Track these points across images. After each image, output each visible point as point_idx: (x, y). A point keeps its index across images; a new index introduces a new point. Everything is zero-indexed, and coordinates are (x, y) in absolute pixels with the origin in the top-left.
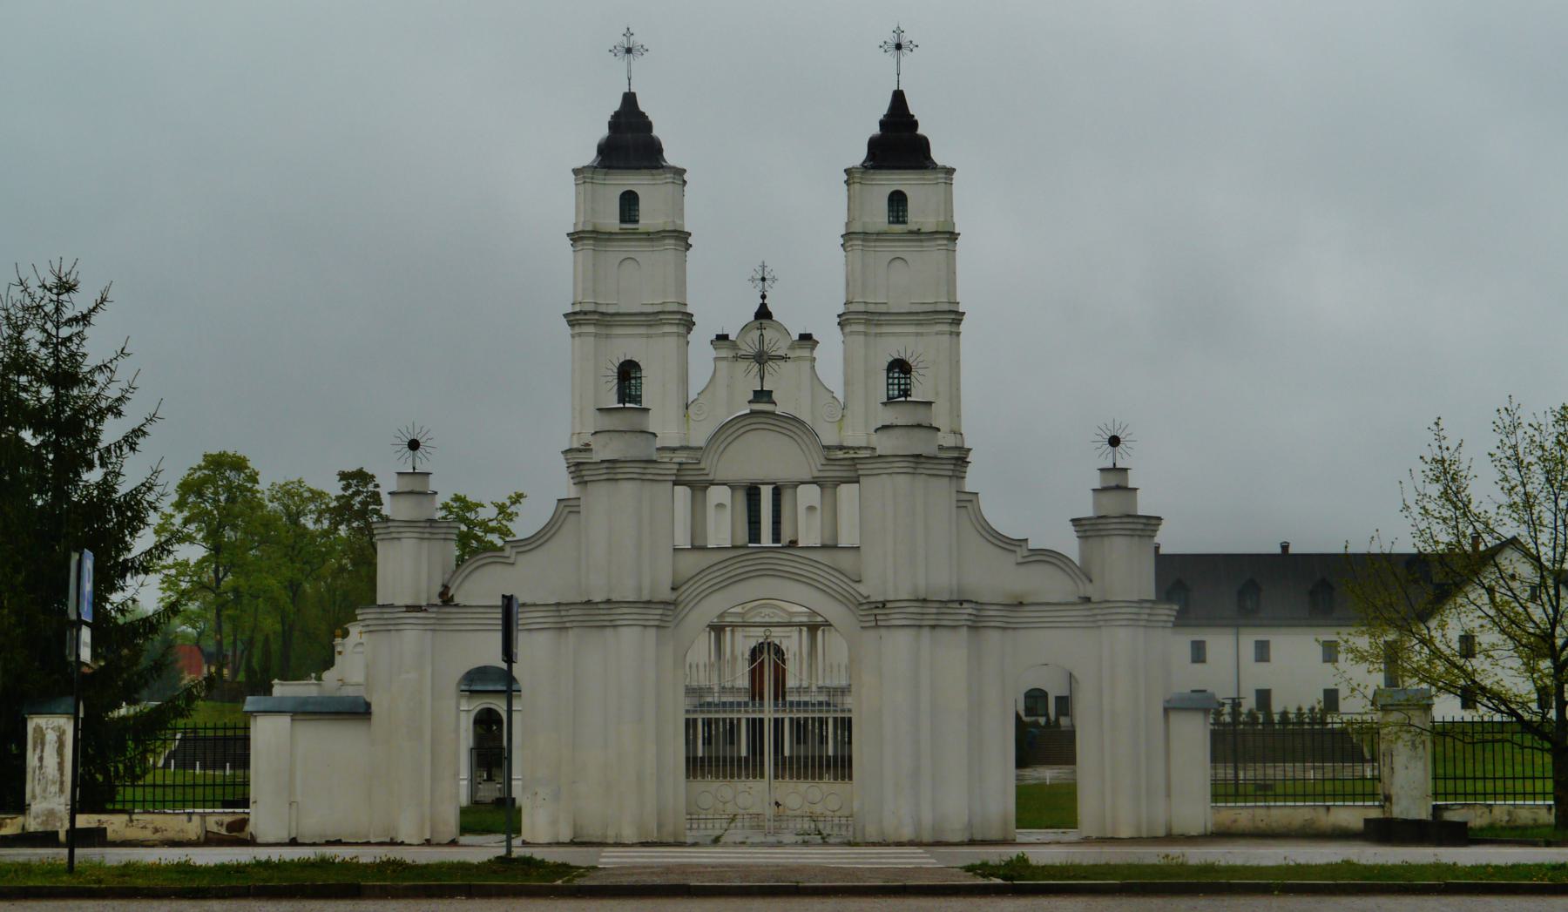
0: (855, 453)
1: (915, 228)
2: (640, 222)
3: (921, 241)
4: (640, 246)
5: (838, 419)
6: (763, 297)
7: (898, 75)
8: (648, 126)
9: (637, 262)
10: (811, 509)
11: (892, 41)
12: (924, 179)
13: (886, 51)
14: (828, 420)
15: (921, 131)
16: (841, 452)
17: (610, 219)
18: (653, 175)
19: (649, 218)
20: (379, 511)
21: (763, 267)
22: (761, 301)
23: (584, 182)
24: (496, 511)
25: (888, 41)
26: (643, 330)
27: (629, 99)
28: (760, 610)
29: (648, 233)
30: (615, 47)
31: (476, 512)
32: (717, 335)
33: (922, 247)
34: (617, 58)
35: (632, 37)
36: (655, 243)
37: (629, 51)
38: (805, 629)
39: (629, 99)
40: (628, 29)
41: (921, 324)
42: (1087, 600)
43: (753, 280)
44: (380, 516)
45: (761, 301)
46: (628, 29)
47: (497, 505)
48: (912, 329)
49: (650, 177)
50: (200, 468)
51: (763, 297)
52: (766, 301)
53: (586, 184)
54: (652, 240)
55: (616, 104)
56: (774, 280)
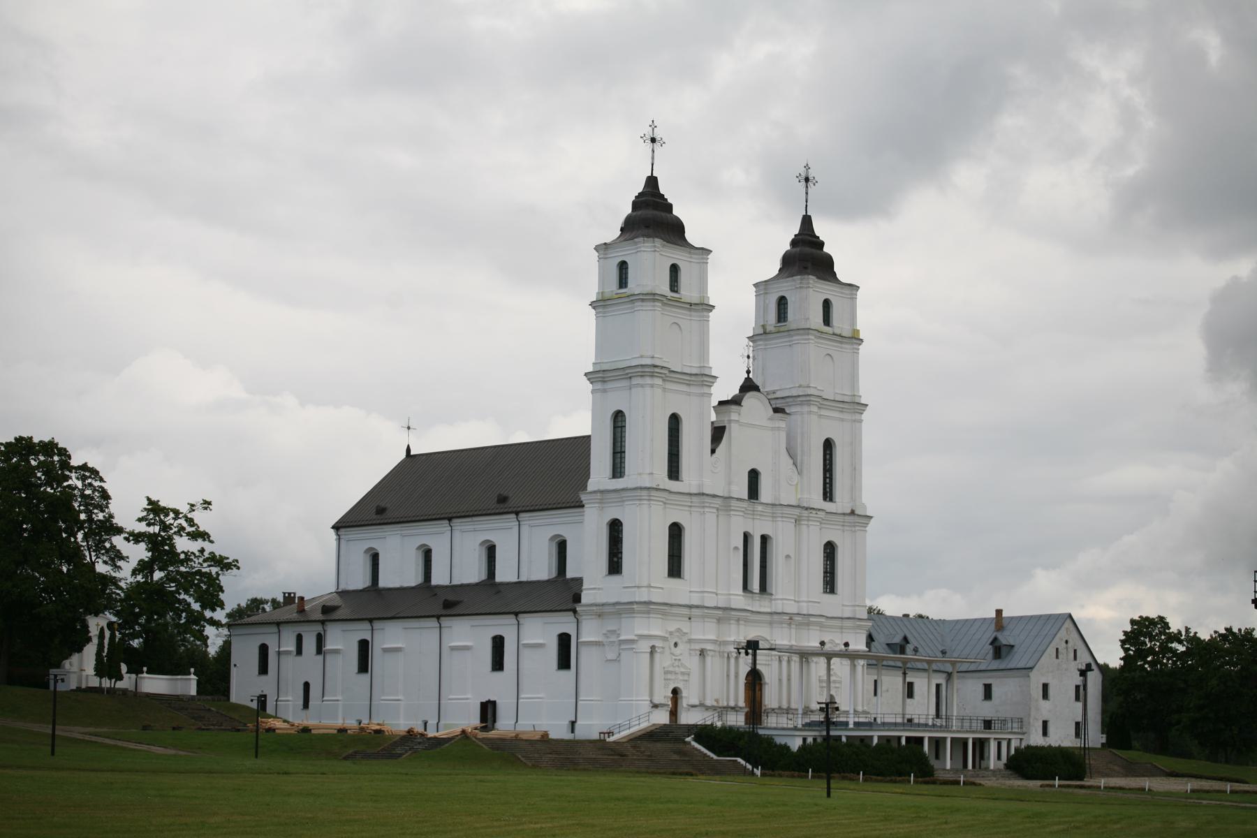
0: (816, 513)
1: (837, 331)
3: (841, 343)
4: (679, 313)
6: (748, 372)
7: (807, 202)
8: (669, 207)
9: (680, 327)
10: (788, 556)
11: (804, 175)
12: (842, 293)
14: (790, 482)
15: (825, 249)
16: (806, 512)
17: (665, 289)
18: (690, 253)
19: (688, 291)
22: (746, 376)
23: (655, 251)
25: (802, 174)
26: (684, 388)
27: (652, 182)
33: (841, 348)
36: (693, 313)
38: (796, 658)
39: (652, 182)
40: (653, 121)
41: (842, 411)
43: (743, 356)
46: (653, 121)
49: (689, 255)
53: (656, 253)
54: (690, 310)
56: (743, 356)
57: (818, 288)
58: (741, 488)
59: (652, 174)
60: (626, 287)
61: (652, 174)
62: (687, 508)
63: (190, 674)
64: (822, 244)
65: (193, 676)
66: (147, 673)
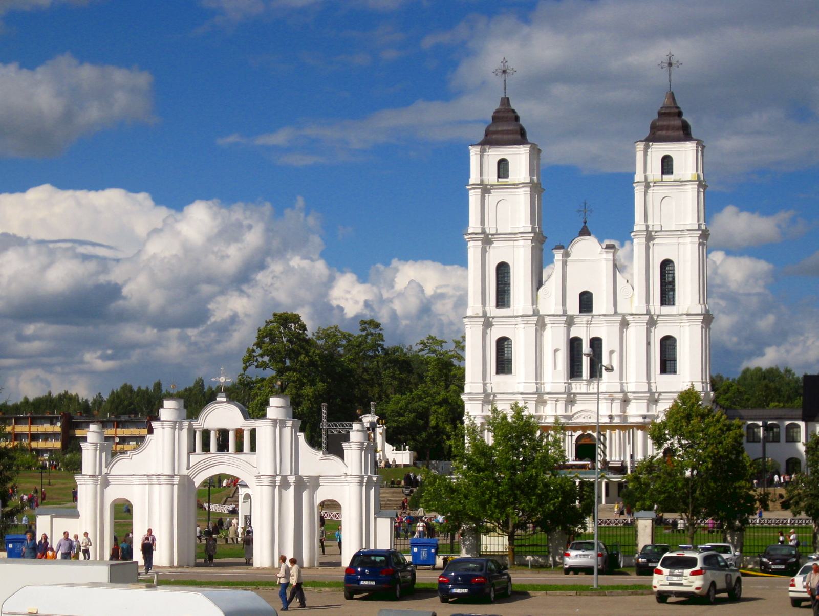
0: (639, 318)
1: (677, 178)
2: (510, 177)
5: (629, 296)
6: (585, 223)
11: (666, 60)
13: (662, 68)
20: (383, 345)
21: (585, 203)
24: (454, 345)
26: (511, 243)
28: (581, 414)
29: (514, 184)
30: (496, 70)
31: (441, 346)
32: (556, 246)
34: (497, 76)
35: (506, 63)
37: (504, 72)
42: (346, 475)
44: (383, 349)
45: (584, 224)
46: (504, 59)
47: (456, 342)
48: (675, 240)
50: (272, 322)
51: (585, 223)
52: (586, 224)
55: (496, 106)
56: (591, 211)
57: (656, 148)
58: (573, 307)
59: (505, 96)
60: (507, 176)
61: (505, 96)
62: (514, 326)
63: (405, 450)
64: (680, 114)
65: (408, 451)
66: (396, 450)
